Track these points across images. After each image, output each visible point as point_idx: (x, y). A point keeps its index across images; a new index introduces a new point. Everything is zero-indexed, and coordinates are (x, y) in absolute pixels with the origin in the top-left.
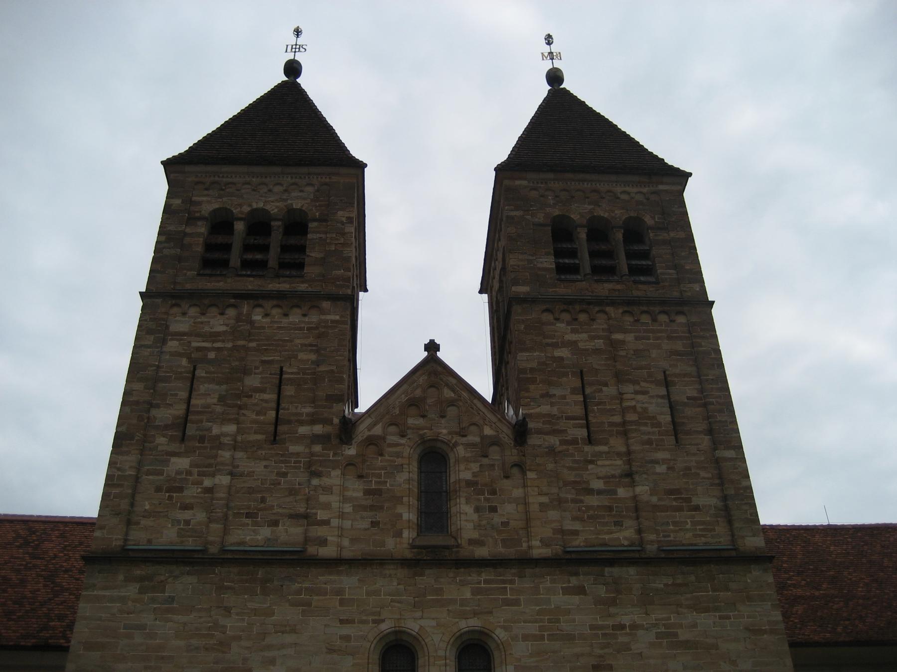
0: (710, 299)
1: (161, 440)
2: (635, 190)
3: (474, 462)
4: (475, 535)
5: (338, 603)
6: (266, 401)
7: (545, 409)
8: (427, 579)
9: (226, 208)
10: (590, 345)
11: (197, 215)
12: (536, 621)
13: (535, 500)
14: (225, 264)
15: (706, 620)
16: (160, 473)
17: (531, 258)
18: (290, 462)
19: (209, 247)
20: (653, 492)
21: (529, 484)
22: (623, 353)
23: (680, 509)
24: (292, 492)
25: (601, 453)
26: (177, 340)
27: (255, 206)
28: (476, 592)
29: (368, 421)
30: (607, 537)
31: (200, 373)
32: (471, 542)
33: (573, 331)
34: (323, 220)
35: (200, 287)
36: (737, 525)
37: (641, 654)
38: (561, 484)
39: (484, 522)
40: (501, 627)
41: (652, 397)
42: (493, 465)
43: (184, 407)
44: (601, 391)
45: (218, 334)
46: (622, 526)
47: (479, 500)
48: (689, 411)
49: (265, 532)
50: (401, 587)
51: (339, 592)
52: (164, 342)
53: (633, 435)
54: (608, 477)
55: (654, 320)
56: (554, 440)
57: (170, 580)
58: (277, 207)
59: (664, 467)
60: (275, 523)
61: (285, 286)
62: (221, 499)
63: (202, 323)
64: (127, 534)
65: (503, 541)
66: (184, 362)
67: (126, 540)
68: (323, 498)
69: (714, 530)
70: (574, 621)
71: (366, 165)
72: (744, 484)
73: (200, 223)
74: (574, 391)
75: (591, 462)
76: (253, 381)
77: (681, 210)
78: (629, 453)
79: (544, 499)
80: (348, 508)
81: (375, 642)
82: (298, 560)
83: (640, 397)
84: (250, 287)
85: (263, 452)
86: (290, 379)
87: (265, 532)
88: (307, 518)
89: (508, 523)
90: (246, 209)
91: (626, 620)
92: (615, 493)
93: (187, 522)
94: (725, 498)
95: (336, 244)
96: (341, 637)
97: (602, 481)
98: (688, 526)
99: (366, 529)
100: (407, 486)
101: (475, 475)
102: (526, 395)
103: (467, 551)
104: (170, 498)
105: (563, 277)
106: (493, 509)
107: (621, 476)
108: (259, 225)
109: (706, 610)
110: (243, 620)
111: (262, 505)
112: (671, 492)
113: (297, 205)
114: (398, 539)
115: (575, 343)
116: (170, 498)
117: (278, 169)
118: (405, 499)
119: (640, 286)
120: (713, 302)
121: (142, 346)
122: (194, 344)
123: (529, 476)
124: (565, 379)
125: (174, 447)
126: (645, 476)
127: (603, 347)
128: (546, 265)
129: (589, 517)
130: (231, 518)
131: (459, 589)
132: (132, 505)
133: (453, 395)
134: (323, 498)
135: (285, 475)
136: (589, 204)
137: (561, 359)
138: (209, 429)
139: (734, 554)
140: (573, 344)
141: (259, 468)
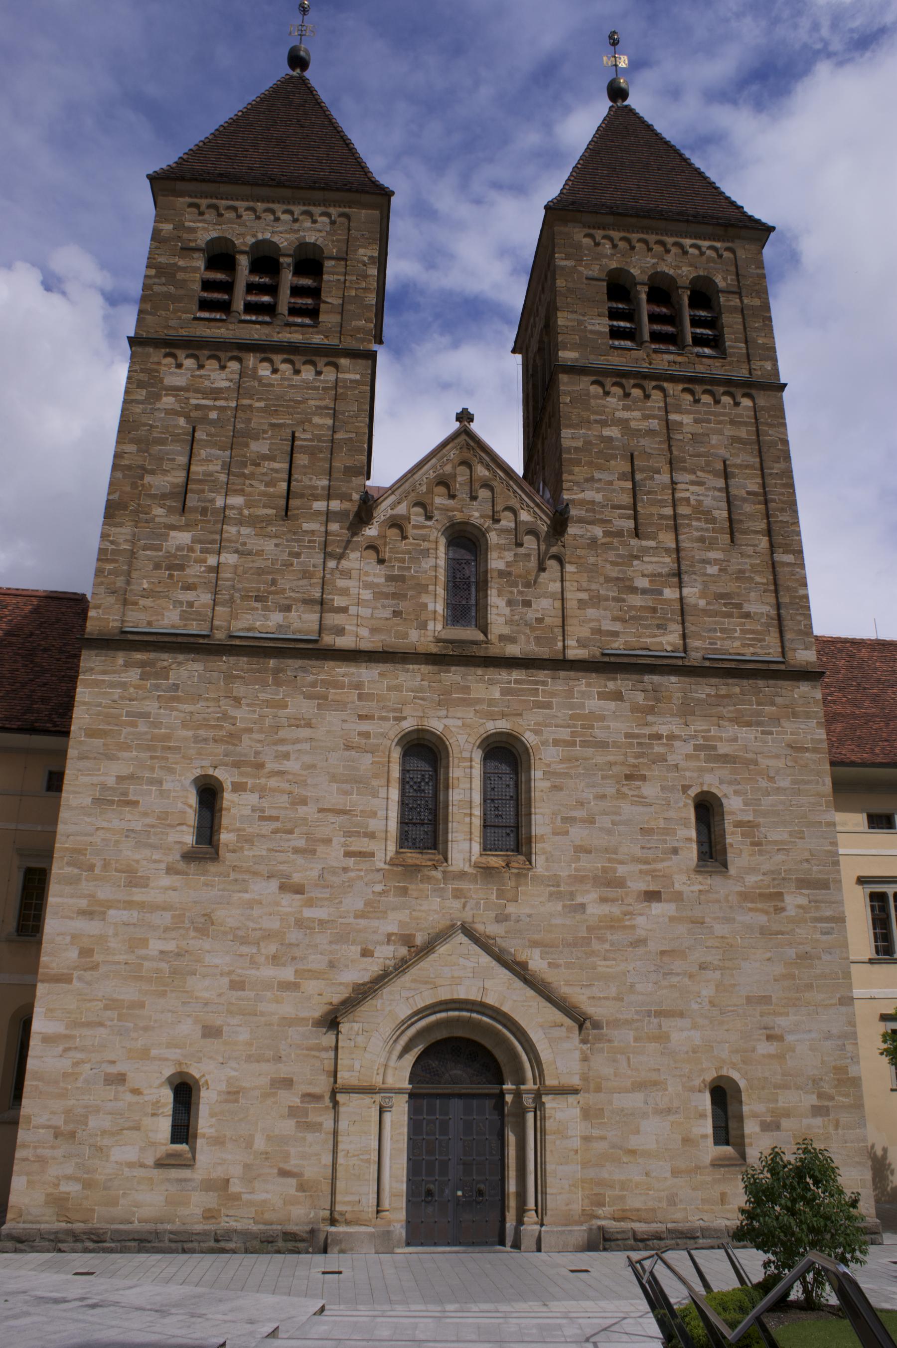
0: (783, 381)
1: (158, 511)
2: (706, 243)
3: (508, 550)
4: (506, 630)
5: (356, 698)
6: (276, 471)
7: (589, 495)
8: (453, 676)
9: (226, 239)
10: (644, 425)
11: (193, 244)
12: (569, 727)
13: (573, 596)
14: (225, 307)
15: (747, 735)
16: (159, 548)
17: (581, 318)
18: (303, 541)
19: (207, 285)
20: (703, 595)
21: (568, 578)
22: (680, 437)
23: (729, 615)
24: (306, 574)
25: (646, 550)
26: (174, 396)
27: (260, 237)
28: (505, 692)
29: (392, 499)
30: (649, 640)
31: (200, 435)
32: (502, 638)
33: (626, 408)
34: (342, 259)
35: (198, 334)
36: (788, 636)
37: (676, 766)
38: (602, 580)
39: (517, 617)
40: (531, 730)
41: (708, 489)
42: (529, 555)
43: (183, 474)
44: (652, 478)
45: (219, 390)
46: (666, 629)
47: (512, 592)
48: (748, 508)
49: (277, 618)
50: (425, 683)
51: (358, 686)
52: (158, 397)
53: (685, 531)
54: (654, 575)
55: (717, 402)
56: (598, 531)
57: (174, 666)
58: (286, 240)
59: (716, 568)
60: (288, 609)
61: (296, 337)
62: (227, 580)
63: (201, 376)
64: (124, 615)
65: (537, 638)
66: (182, 421)
67: (123, 621)
68: (341, 583)
69: (764, 640)
70: (608, 727)
71: (393, 193)
72: (801, 592)
73: (196, 255)
74: (622, 477)
75: (637, 557)
76: (259, 447)
77: (759, 271)
78: (678, 550)
79: (584, 596)
80: (367, 595)
81: (396, 740)
82: (314, 651)
83: (693, 488)
84: (256, 337)
85: (274, 529)
86: (302, 447)
87: (277, 618)
88: (322, 604)
89: (543, 619)
90: (250, 240)
91: (664, 730)
92: (661, 593)
93: (190, 604)
94: (778, 606)
95: (356, 289)
96: (360, 734)
97: (646, 580)
98: (736, 635)
99: (387, 619)
100: (434, 574)
101: (508, 564)
102: (570, 478)
103: (495, 650)
104: (171, 576)
105: (616, 343)
106: (527, 604)
107: (669, 575)
108: (265, 261)
109: (749, 724)
110: (255, 711)
111: (273, 588)
112: (722, 596)
113: (311, 238)
114: (423, 631)
115: (627, 420)
116: (171, 576)
117: (287, 192)
118: (431, 588)
119: (704, 360)
120: (785, 385)
121: (132, 401)
122: (194, 401)
123: (567, 570)
124: (613, 462)
125: (174, 519)
126: (694, 577)
127: (657, 428)
128: (597, 328)
129: (631, 618)
130: (238, 601)
131: (487, 687)
132: (128, 583)
133: (487, 473)
134: (341, 583)
135: (298, 555)
136: (652, 257)
137: (610, 439)
138: (213, 501)
139: (782, 667)
140: (624, 424)
141: (269, 546)
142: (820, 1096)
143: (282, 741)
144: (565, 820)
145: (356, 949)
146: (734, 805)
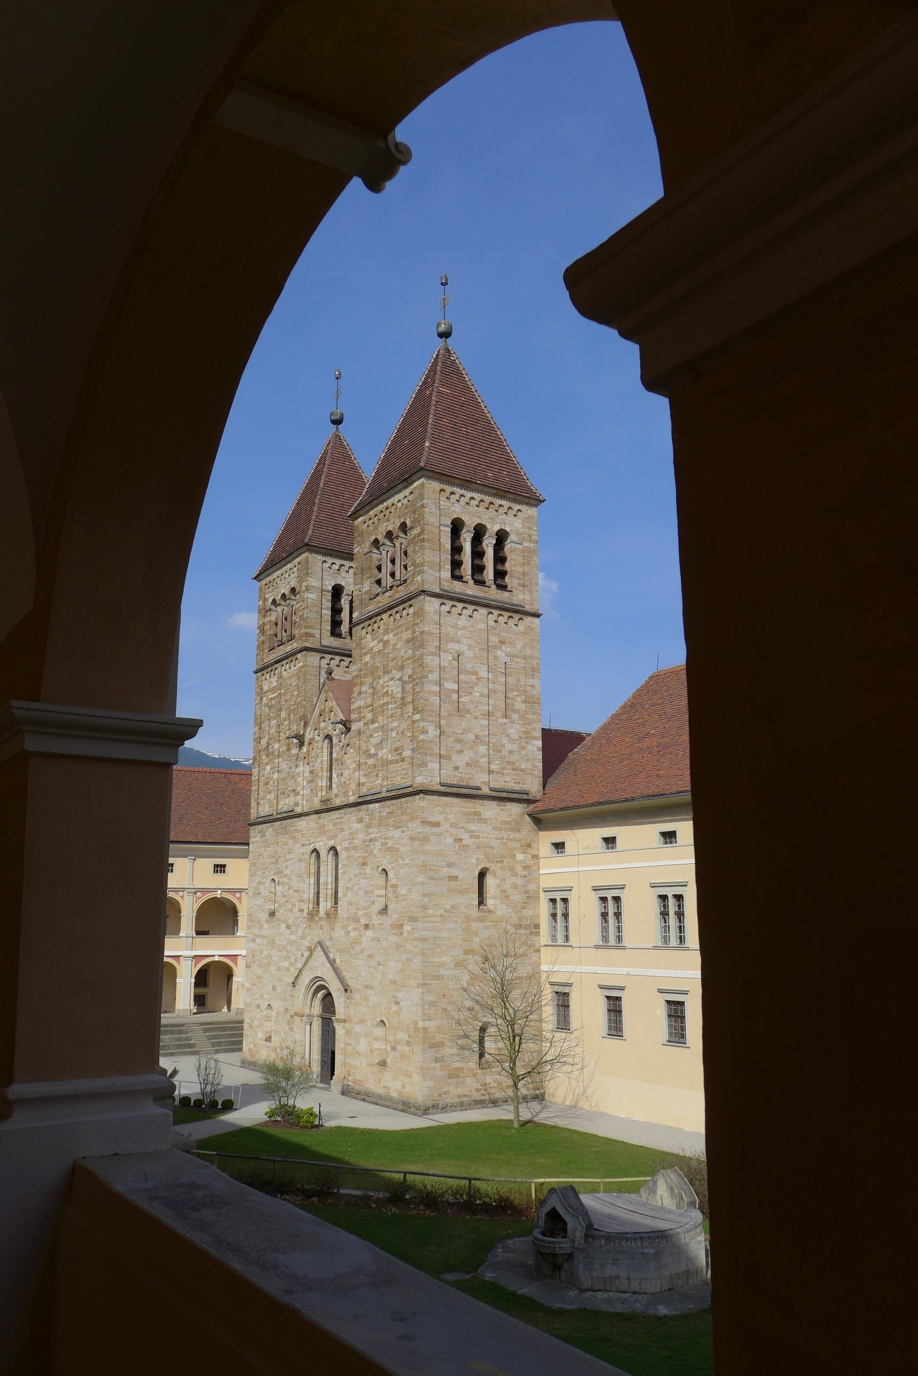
28: (334, 824)
32: (336, 795)
91: (372, 836)
142: (409, 1036)
143: (286, 861)
144: (347, 888)
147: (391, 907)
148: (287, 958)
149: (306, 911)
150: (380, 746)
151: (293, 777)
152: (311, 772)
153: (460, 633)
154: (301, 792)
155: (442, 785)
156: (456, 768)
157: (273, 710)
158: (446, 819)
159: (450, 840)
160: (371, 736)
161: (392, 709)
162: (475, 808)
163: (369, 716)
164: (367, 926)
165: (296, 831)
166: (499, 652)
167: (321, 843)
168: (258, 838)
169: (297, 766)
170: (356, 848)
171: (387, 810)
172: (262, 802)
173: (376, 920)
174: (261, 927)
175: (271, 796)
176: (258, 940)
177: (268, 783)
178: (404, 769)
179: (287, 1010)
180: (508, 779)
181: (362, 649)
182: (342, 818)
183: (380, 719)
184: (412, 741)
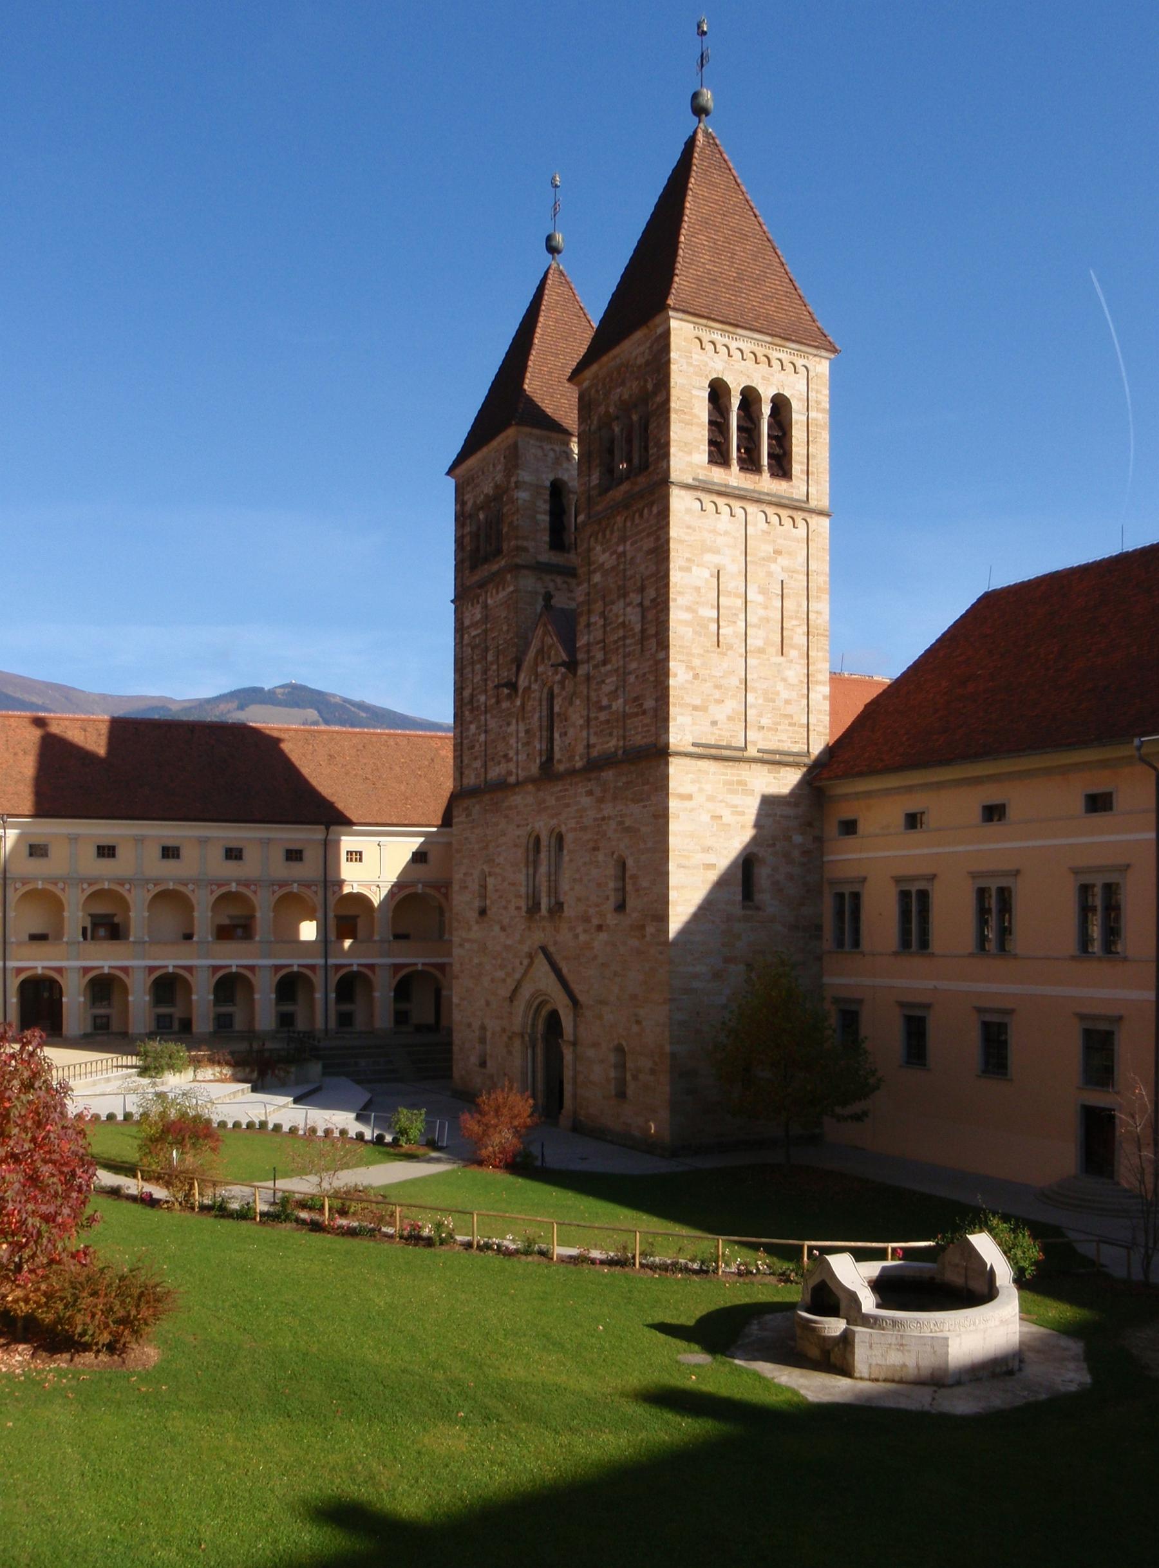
20: (625, 703)
28: (558, 799)
91: (606, 813)
106: (565, 734)
144: (575, 880)
145: (517, 962)
146: (630, 862)
147: (630, 904)
148: (502, 967)
149: (524, 909)
150: (613, 695)
151: (504, 738)
152: (527, 732)
153: (721, 540)
154: (515, 758)
155: (694, 745)
156: (714, 723)
157: (477, 651)
158: (701, 790)
159: (705, 818)
160: (603, 682)
161: (630, 645)
162: (739, 775)
163: (600, 656)
164: (600, 928)
165: (510, 808)
166: (773, 567)
167: (541, 823)
168: (463, 818)
169: (509, 724)
170: (584, 829)
171: (624, 779)
172: (466, 772)
173: (611, 919)
174: (470, 929)
175: (478, 764)
176: (467, 946)
177: (473, 747)
178: (647, 725)
179: (504, 1030)
180: (784, 737)
181: (589, 564)
182: (566, 790)
183: (614, 659)
184: (655, 687)
